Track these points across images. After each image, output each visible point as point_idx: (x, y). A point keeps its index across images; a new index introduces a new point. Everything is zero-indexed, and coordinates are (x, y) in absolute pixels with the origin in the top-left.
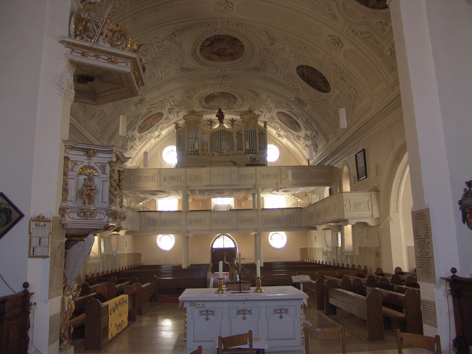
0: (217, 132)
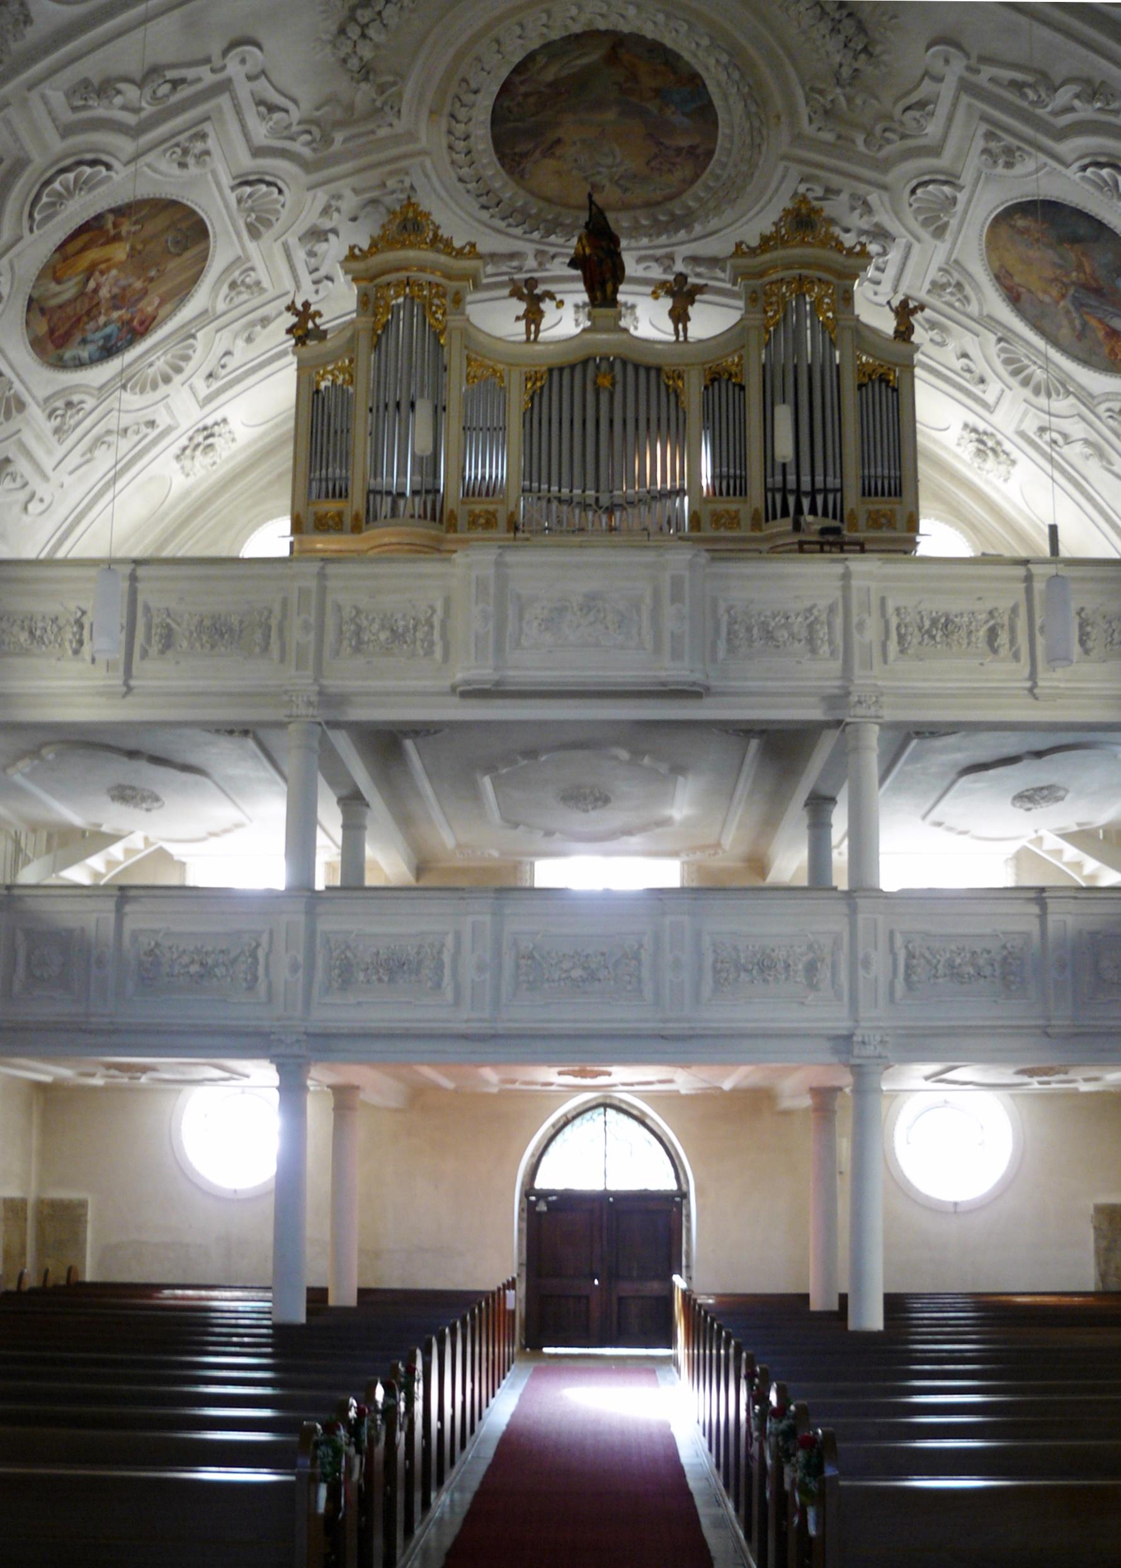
0: (572, 367)
